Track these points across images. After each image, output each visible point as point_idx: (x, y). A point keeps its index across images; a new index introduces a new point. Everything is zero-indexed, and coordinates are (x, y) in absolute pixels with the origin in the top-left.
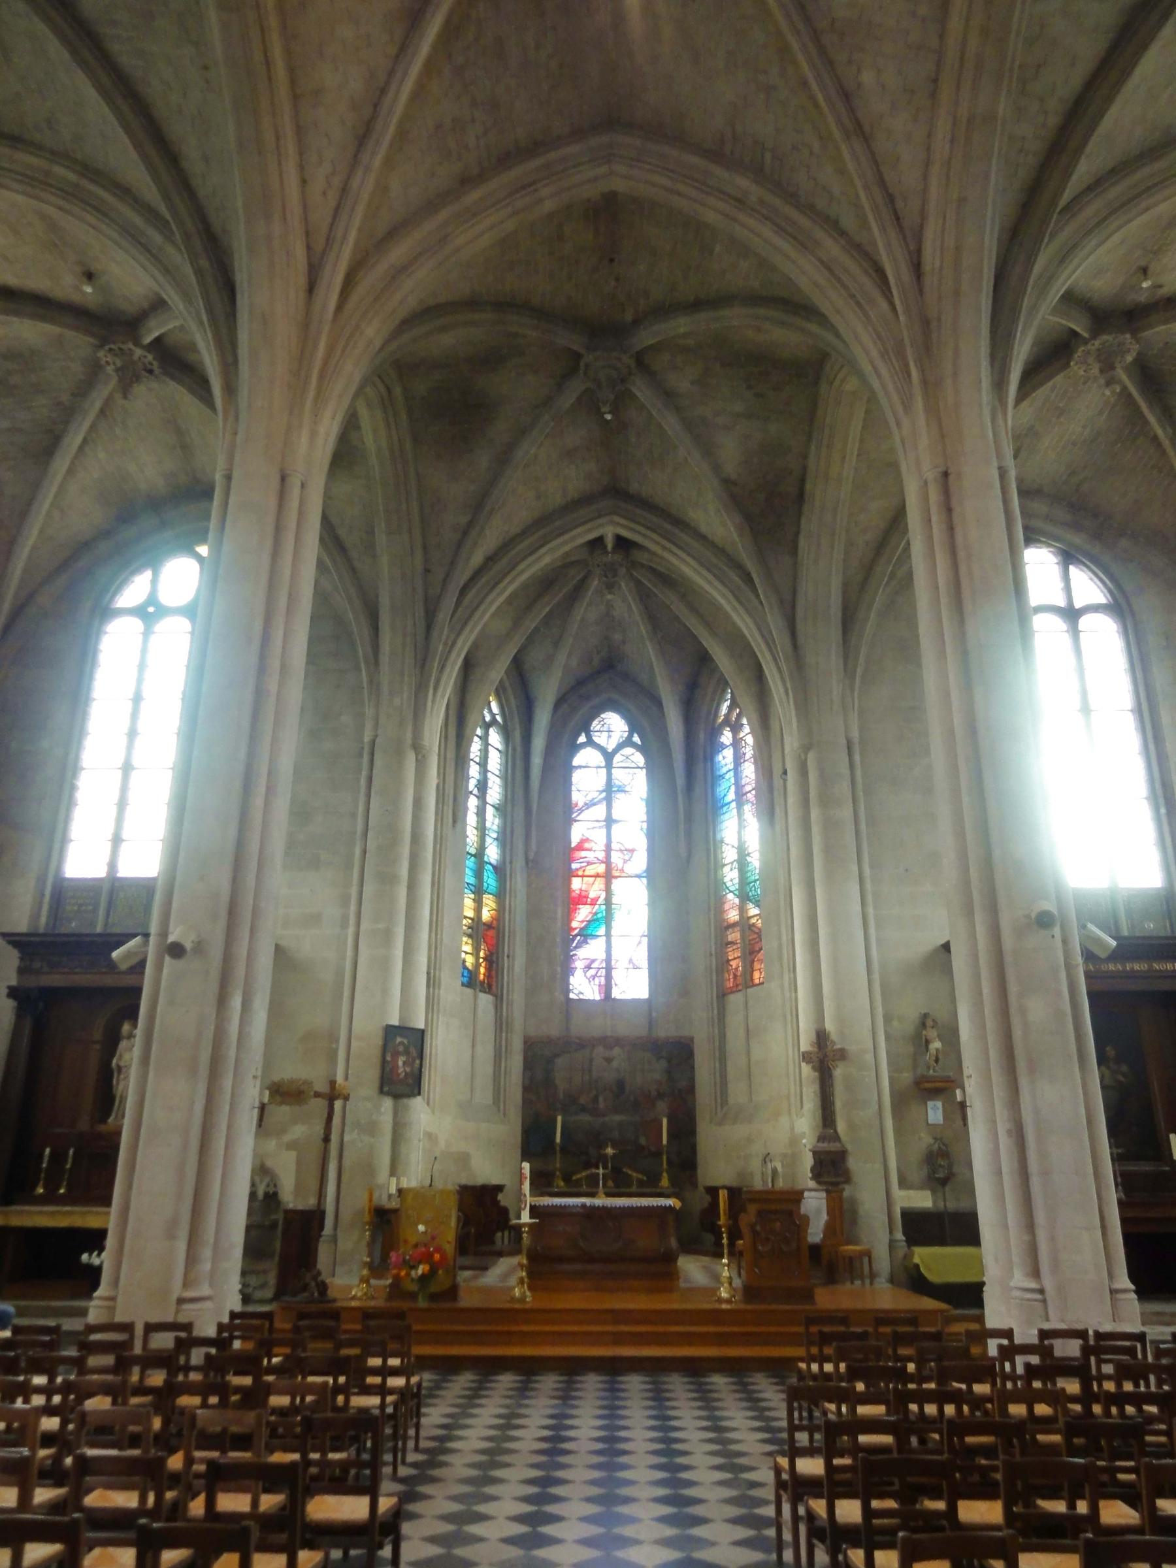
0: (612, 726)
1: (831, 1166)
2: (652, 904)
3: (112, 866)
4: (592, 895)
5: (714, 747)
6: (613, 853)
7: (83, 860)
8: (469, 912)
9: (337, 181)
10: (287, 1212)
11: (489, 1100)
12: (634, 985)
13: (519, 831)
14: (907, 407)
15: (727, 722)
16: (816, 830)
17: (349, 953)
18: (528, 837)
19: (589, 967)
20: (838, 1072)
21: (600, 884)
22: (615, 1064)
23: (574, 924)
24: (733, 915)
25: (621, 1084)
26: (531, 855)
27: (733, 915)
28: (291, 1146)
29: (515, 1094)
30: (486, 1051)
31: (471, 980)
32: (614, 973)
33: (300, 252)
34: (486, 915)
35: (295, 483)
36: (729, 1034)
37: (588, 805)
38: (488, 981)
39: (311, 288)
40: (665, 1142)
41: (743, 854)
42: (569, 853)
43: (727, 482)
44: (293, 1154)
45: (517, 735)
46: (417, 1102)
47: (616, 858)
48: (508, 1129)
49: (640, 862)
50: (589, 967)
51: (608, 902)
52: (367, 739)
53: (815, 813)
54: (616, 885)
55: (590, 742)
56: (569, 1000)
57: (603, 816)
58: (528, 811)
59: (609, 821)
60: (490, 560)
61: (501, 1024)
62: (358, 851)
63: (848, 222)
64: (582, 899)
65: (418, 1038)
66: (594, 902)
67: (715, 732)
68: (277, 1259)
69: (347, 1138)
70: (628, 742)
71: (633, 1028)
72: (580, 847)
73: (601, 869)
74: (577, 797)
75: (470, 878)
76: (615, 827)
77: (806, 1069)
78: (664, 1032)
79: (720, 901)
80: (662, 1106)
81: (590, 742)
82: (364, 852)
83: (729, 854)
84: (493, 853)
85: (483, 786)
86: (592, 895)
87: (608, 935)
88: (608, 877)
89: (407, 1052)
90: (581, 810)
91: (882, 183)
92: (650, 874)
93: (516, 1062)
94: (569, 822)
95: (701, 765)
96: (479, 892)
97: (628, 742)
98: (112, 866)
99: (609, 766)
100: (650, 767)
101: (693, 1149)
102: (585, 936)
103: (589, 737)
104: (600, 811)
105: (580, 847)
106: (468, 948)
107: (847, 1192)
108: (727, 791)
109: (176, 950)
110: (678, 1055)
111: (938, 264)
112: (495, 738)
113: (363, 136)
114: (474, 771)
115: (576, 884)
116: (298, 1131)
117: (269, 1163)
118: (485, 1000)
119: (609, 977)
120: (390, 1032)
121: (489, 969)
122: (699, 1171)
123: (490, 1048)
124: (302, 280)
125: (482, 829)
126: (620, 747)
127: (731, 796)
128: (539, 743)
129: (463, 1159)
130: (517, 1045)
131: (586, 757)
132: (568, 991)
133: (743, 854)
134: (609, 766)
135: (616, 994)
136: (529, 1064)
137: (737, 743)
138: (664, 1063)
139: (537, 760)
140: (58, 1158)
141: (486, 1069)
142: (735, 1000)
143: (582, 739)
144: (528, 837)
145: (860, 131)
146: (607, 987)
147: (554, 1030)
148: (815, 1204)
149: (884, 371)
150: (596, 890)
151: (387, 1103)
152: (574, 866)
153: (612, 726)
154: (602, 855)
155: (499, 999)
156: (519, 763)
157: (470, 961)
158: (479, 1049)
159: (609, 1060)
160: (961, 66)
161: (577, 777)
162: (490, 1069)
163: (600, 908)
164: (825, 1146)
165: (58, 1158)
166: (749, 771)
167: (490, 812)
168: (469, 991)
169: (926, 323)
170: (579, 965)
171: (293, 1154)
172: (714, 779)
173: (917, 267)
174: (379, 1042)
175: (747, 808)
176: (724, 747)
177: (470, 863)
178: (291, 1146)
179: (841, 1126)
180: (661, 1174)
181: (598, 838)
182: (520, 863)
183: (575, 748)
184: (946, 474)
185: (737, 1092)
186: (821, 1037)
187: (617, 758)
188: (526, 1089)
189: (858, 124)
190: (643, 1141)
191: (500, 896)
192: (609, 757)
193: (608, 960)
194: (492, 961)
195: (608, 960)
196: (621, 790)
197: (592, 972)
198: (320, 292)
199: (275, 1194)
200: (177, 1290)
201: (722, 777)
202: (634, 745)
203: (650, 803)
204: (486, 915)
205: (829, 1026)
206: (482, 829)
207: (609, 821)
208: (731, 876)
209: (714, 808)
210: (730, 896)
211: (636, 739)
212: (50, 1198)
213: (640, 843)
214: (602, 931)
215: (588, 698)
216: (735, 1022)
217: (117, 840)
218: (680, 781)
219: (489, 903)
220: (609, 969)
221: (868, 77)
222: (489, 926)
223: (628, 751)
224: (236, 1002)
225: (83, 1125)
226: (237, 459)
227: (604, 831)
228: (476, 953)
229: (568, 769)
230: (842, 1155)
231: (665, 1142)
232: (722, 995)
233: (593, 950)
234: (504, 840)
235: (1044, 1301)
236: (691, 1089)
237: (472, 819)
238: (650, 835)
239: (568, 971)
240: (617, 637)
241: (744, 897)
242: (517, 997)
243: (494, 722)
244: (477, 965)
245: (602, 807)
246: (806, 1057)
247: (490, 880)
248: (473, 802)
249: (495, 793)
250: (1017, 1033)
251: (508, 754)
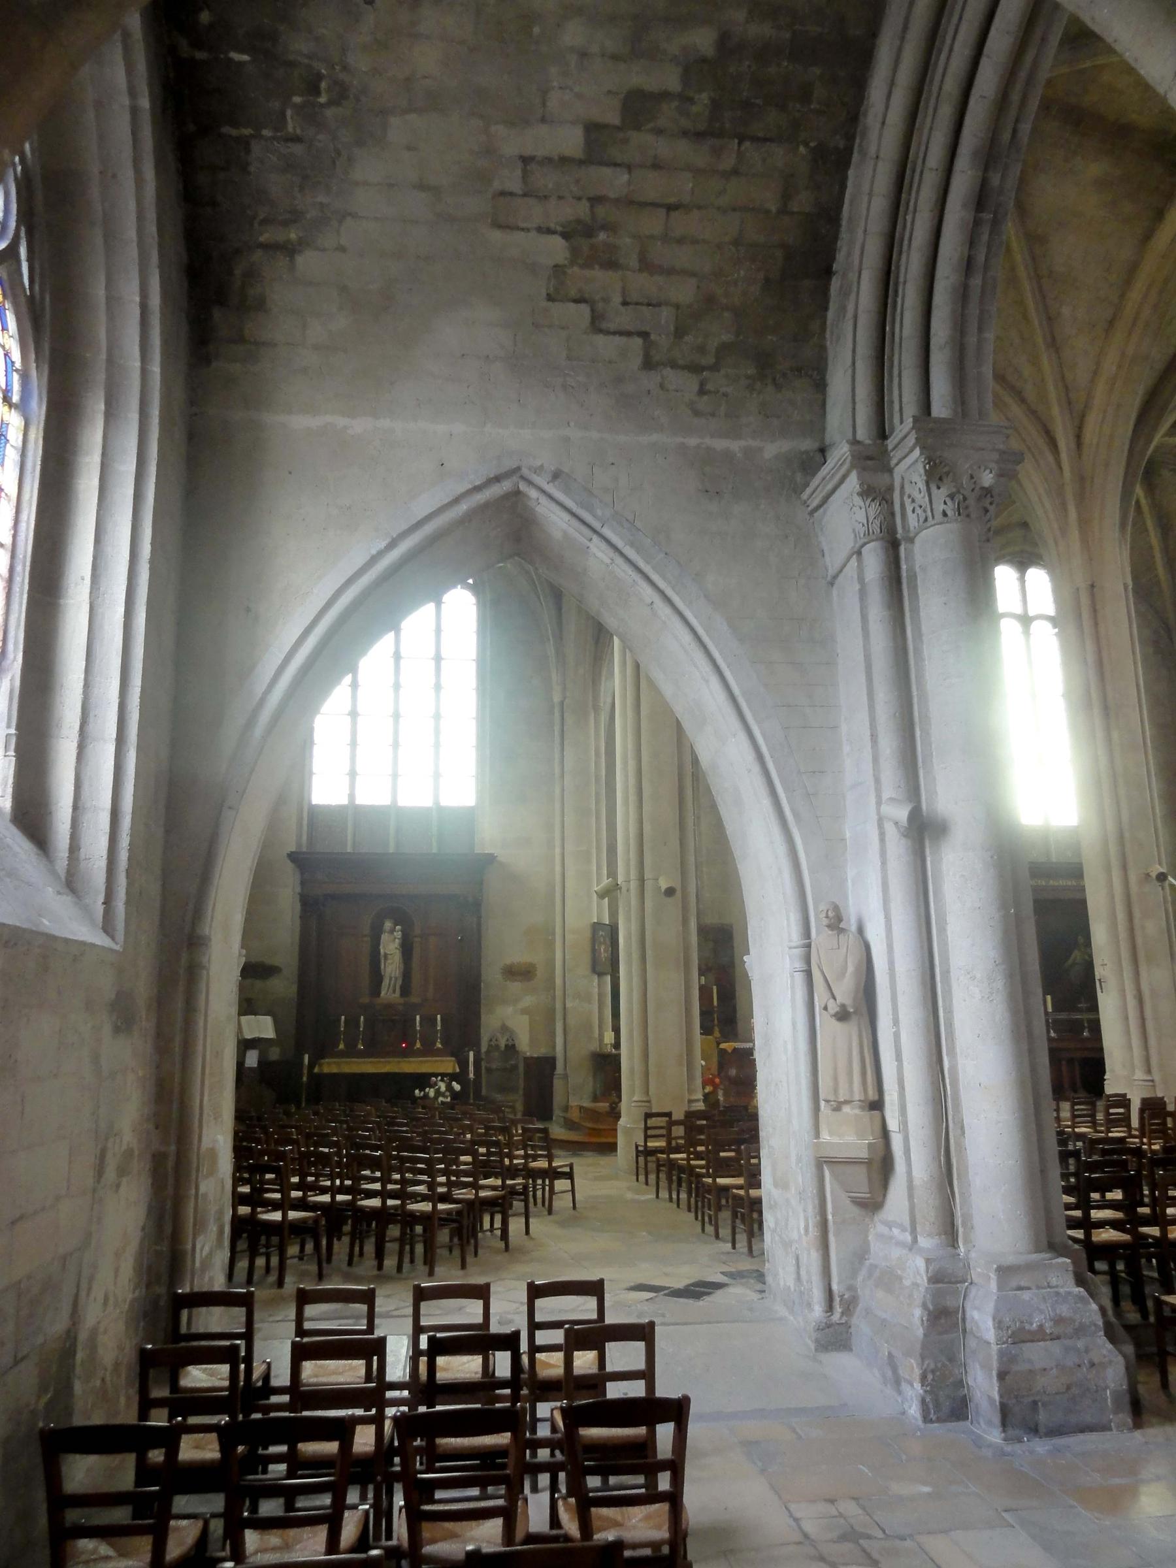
3: (352, 796)
7: (326, 789)
10: (526, 1059)
14: (1064, 531)
17: (558, 868)
28: (525, 1011)
40: (715, 1003)
44: (525, 1019)
52: (557, 698)
62: (558, 791)
63: (1030, 393)
68: (521, 1092)
69: (569, 1005)
82: (563, 790)
91: (1063, 378)
98: (352, 796)
101: (734, 1010)
111: (1095, 442)
116: (528, 1001)
117: (509, 1023)
140: (352, 1022)
145: (1054, 344)
149: (1048, 505)
160: (1134, 324)
165: (352, 1022)
169: (1082, 479)
171: (526, 1017)
173: (1079, 437)
174: (588, 934)
178: (525, 1011)
180: (713, 1027)
184: (1092, 586)
189: (1054, 339)
199: (514, 1046)
200: (687, 1097)
212: (351, 1052)
217: (353, 774)
221: (1066, 311)
225: (365, 1000)
231: (715, 1003)
235: (1154, 1086)
250: (1139, 941)
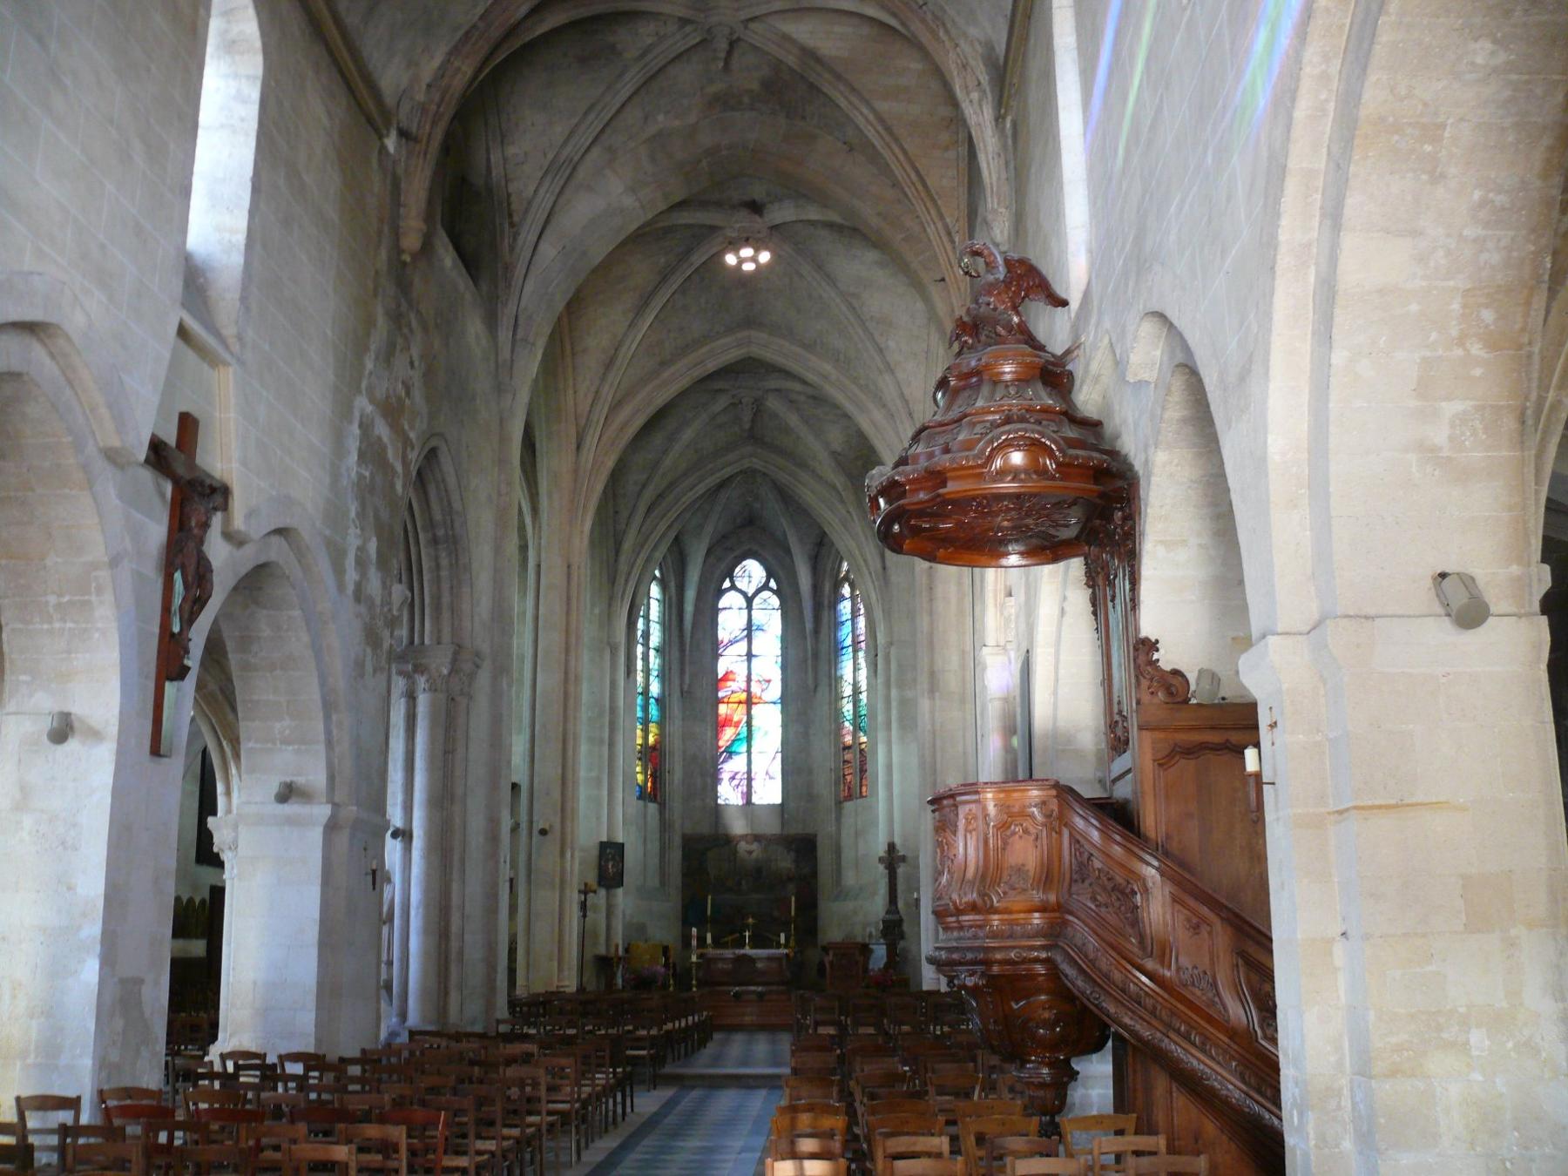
0: (752, 572)
1: (894, 929)
2: (785, 726)
4: (736, 719)
5: (839, 598)
6: (753, 684)
8: (639, 741)
9: (593, 389)
11: (654, 881)
12: (769, 792)
13: (675, 667)
15: (846, 578)
16: (894, 704)
18: (682, 672)
19: (733, 778)
20: (901, 870)
21: (743, 708)
22: (754, 855)
23: (721, 743)
24: (848, 739)
25: (759, 870)
26: (686, 688)
27: (848, 739)
29: (676, 877)
30: (654, 847)
31: (643, 795)
32: (754, 783)
33: (573, 432)
34: (651, 740)
35: (574, 567)
36: (844, 834)
37: (731, 643)
38: (654, 794)
39: (578, 448)
41: (856, 691)
42: (717, 683)
43: (834, 454)
45: (672, 585)
46: (620, 891)
47: (755, 689)
48: (672, 904)
49: (775, 691)
50: (733, 778)
51: (749, 724)
53: (894, 692)
54: (755, 710)
55: (733, 587)
56: (717, 805)
57: (744, 652)
58: (682, 651)
59: (750, 656)
60: (661, 496)
61: (665, 825)
64: (727, 722)
65: (620, 847)
66: (737, 724)
67: (837, 585)
70: (765, 587)
71: (772, 827)
72: (726, 678)
73: (743, 696)
74: (723, 634)
75: (639, 714)
76: (754, 660)
77: (881, 867)
78: (795, 829)
79: (840, 727)
80: (791, 887)
81: (733, 587)
83: (847, 690)
84: (655, 689)
85: (646, 635)
86: (736, 719)
87: (749, 752)
88: (749, 702)
89: (613, 858)
90: (726, 647)
92: (784, 700)
93: (676, 856)
94: (716, 656)
95: (825, 614)
96: (646, 722)
97: (765, 587)
99: (749, 607)
100: (783, 607)
101: (815, 919)
102: (730, 754)
103: (732, 582)
104: (742, 647)
105: (726, 678)
106: (638, 769)
107: (902, 944)
108: (845, 633)
109: (543, 832)
110: (804, 847)
112: (655, 590)
113: (609, 365)
114: (640, 624)
115: (723, 709)
118: (653, 807)
119: (749, 786)
120: (604, 846)
121: (654, 783)
122: (820, 936)
123: (657, 844)
124: (574, 446)
125: (647, 671)
126: (758, 591)
127: (848, 642)
128: (690, 595)
129: (641, 929)
130: (677, 841)
131: (730, 600)
132: (717, 797)
133: (856, 691)
134: (749, 607)
135: (756, 799)
136: (686, 857)
137: (853, 598)
138: (793, 854)
139: (689, 608)
141: (654, 861)
142: (848, 805)
143: (727, 584)
144: (682, 672)
146: (748, 795)
147: (705, 829)
148: (880, 952)
150: (739, 714)
151: (602, 892)
152: (721, 694)
153: (752, 572)
154: (743, 686)
155: (662, 806)
156: (674, 611)
157: (640, 778)
158: (649, 846)
159: (750, 853)
161: (722, 617)
162: (657, 860)
163: (743, 730)
164: (890, 917)
166: (862, 622)
167: (652, 653)
168: (641, 803)
170: (725, 776)
172: (838, 624)
175: (861, 654)
176: (843, 598)
177: (639, 700)
179: (901, 905)
181: (740, 670)
182: (676, 694)
183: (720, 593)
185: (850, 878)
186: (891, 847)
187: (757, 601)
188: (684, 875)
190: (776, 914)
191: (661, 724)
192: (749, 601)
193: (749, 772)
194: (657, 776)
195: (749, 772)
196: (759, 629)
197: (735, 782)
198: (584, 451)
201: (843, 623)
202: (771, 590)
203: (784, 639)
204: (651, 740)
205: (897, 840)
206: (647, 671)
207: (750, 656)
208: (847, 708)
209: (837, 649)
210: (847, 724)
211: (773, 584)
213: (776, 675)
214: (744, 748)
215: (732, 549)
216: (848, 821)
218: (809, 626)
219: (653, 728)
220: (750, 780)
221: (891, 344)
222: (654, 748)
223: (766, 594)
224: (568, 855)
226: (543, 555)
227: (745, 664)
228: (645, 772)
229: (715, 611)
230: (901, 920)
232: (839, 803)
233: (736, 765)
234: (663, 676)
236: (814, 874)
237: (640, 664)
238: (784, 668)
239: (716, 780)
240: (757, 505)
241: (857, 728)
242: (676, 806)
243: (655, 578)
244: (646, 781)
245: (744, 644)
246: (881, 860)
247: (654, 711)
248: (640, 649)
249: (655, 639)
251: (665, 602)
